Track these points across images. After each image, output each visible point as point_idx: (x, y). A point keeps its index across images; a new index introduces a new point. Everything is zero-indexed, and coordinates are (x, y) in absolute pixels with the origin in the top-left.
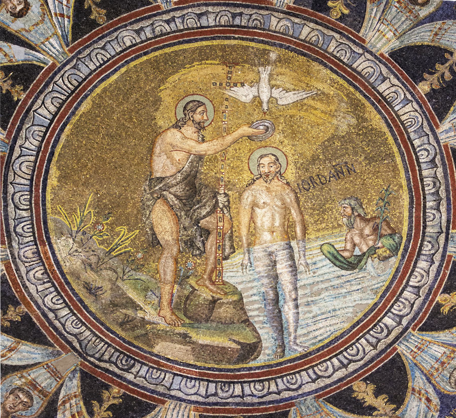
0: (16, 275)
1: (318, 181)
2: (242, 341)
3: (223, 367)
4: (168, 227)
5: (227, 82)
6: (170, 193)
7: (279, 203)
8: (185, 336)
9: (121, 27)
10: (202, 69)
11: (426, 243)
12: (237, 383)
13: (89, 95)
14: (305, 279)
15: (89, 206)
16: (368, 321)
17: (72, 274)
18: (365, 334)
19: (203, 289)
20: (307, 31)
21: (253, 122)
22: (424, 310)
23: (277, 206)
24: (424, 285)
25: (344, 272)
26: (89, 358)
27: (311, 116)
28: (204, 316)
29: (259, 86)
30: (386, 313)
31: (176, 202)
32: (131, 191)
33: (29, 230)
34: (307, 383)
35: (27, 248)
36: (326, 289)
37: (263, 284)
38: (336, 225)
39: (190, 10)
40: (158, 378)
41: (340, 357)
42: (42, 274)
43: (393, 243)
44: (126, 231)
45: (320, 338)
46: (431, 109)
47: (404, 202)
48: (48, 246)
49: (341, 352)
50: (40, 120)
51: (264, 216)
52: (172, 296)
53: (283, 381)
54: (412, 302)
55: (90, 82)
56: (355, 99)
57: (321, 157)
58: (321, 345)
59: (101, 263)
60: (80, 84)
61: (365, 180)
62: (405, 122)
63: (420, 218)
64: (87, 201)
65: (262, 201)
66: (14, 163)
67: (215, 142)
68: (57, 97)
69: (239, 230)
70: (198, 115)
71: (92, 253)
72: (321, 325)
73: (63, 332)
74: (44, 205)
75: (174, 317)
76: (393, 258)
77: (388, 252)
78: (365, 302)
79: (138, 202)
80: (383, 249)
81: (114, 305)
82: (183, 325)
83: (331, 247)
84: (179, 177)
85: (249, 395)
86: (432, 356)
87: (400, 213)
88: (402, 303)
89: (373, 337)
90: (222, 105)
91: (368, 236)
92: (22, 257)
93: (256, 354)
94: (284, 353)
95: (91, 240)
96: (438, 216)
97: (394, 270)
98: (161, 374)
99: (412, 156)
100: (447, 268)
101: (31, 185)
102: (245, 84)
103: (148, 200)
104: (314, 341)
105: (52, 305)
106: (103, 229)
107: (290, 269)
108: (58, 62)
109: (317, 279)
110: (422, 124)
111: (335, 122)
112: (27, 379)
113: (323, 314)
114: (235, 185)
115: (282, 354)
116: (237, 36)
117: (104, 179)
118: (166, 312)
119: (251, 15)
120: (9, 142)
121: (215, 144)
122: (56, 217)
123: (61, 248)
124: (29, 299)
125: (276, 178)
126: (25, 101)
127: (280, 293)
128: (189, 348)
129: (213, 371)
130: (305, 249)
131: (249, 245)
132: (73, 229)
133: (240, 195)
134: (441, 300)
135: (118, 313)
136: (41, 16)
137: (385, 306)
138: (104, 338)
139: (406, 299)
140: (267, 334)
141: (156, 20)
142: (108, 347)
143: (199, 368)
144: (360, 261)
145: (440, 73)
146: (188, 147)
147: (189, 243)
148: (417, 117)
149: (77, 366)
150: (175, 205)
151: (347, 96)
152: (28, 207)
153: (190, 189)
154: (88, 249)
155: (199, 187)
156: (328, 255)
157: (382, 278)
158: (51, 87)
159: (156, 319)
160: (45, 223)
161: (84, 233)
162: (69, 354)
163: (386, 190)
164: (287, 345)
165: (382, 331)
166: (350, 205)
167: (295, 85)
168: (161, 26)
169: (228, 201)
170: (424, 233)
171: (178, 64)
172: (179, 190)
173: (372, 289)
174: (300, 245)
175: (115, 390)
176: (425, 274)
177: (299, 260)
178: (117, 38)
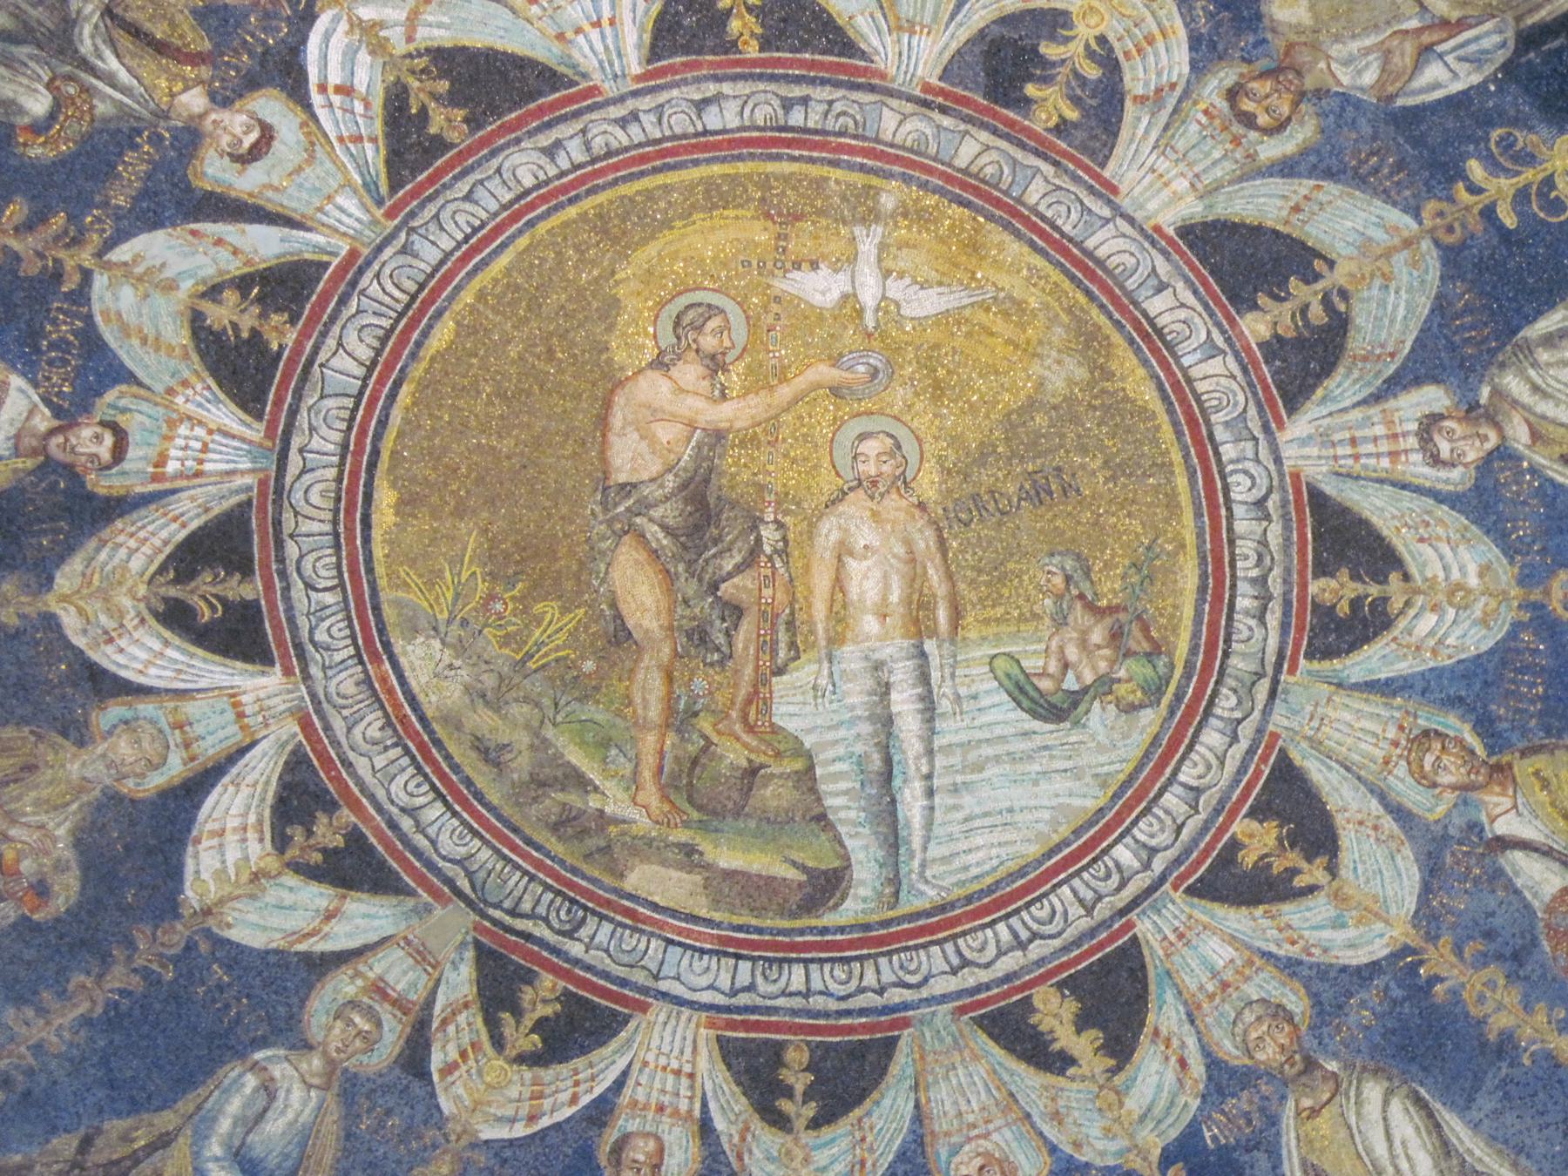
2: (810, 864)
3: (769, 923)
4: (649, 601)
6: (651, 520)
7: (900, 550)
8: (689, 850)
9: (507, 145)
11: (1224, 691)
12: (798, 960)
14: (950, 731)
18: (1072, 876)
20: (973, 149)
21: (841, 355)
25: (1037, 725)
26: (491, 911)
27: (981, 349)
28: (730, 805)
30: (1122, 836)
35: (343, 675)
36: (997, 759)
39: (675, 92)
41: (1014, 921)
42: (382, 729)
45: (975, 871)
49: (1017, 911)
51: (865, 577)
55: (446, 279)
58: (976, 887)
60: (422, 286)
67: (752, 400)
71: (484, 667)
72: (980, 841)
73: (435, 857)
74: (370, 570)
75: (666, 807)
76: (1149, 711)
78: (1077, 802)
82: (686, 825)
84: (670, 482)
86: (1204, 961)
91: (1099, 647)
96: (1259, 633)
97: (1147, 738)
100: (1264, 759)
101: (336, 535)
103: (604, 538)
104: (962, 876)
105: (406, 798)
109: (979, 735)
111: (1036, 369)
112: (364, 977)
113: (986, 814)
114: (798, 504)
116: (797, 153)
118: (650, 795)
119: (830, 103)
122: (400, 594)
124: (356, 790)
127: (896, 758)
133: (812, 525)
137: (1119, 818)
139: (1167, 812)
144: (1075, 705)
146: (687, 413)
151: (1069, 311)
156: (1006, 682)
157: (1122, 753)
159: (631, 812)
160: (377, 609)
161: (464, 623)
163: (1149, 548)
165: (1108, 876)
168: (605, 133)
169: (785, 539)
172: (669, 512)
175: (547, 980)
176: (1214, 762)
178: (498, 171)
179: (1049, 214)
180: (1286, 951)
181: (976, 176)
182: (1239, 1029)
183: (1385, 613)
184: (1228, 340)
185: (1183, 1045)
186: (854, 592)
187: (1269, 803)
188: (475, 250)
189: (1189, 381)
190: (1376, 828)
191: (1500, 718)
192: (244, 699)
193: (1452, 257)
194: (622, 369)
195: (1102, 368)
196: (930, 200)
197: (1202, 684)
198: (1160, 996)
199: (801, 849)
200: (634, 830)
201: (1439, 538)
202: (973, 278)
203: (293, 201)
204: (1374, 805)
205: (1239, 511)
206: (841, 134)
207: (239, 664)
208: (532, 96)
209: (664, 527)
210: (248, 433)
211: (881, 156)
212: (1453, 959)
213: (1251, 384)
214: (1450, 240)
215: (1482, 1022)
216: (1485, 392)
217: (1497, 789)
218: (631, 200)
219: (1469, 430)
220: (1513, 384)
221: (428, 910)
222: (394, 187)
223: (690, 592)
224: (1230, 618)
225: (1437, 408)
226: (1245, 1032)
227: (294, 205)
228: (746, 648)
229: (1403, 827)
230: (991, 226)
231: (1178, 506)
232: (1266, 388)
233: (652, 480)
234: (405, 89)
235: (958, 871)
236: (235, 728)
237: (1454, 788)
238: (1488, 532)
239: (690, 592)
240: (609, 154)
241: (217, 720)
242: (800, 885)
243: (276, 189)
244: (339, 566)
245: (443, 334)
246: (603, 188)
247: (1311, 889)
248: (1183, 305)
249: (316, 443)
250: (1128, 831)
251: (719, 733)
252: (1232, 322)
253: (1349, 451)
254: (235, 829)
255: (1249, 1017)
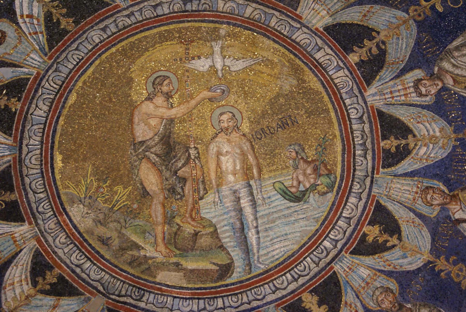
0: (47, 246)
1: (268, 132)
3: (208, 285)
4: (154, 181)
5: (186, 57)
6: (151, 153)
7: (238, 151)
8: (177, 265)
9: (89, 29)
10: (163, 49)
11: (355, 183)
12: (220, 297)
13: (73, 89)
14: (262, 210)
15: (90, 176)
16: (312, 244)
17: (87, 232)
18: (310, 254)
19: (186, 225)
21: (211, 87)
22: (354, 237)
23: (237, 153)
24: (354, 217)
25: (292, 204)
26: (111, 296)
27: (259, 78)
28: (190, 247)
29: (213, 58)
30: (325, 238)
31: (157, 160)
32: (120, 156)
33: (48, 207)
34: (269, 294)
36: (279, 218)
37: (231, 216)
38: (284, 167)
40: (162, 302)
43: (330, 181)
44: (122, 189)
45: (277, 257)
46: (360, 76)
47: (337, 148)
48: (65, 215)
49: (293, 269)
50: (37, 119)
51: (227, 162)
52: (164, 234)
53: (251, 292)
54: (345, 230)
55: (72, 78)
56: (295, 64)
57: (269, 112)
58: (278, 262)
59: (107, 218)
60: (63, 82)
61: (306, 130)
62: (338, 84)
63: (351, 163)
64: (88, 172)
65: (225, 151)
66: (24, 160)
67: (182, 107)
68: (47, 98)
69: (209, 175)
70: (165, 87)
71: (99, 212)
72: (277, 246)
74: (55, 184)
75: (168, 251)
76: (330, 194)
77: (326, 188)
78: (308, 228)
79: (127, 164)
80: (322, 186)
81: (123, 249)
82: (175, 256)
83: (281, 184)
84: (157, 139)
85: (229, 307)
87: (335, 157)
88: (337, 230)
89: (316, 256)
90: (184, 76)
91: (310, 175)
92: (48, 230)
93: (230, 272)
94: (251, 270)
95: (97, 202)
97: (330, 203)
98: (164, 299)
99: (344, 112)
100: (371, 205)
101: (42, 172)
102: (202, 57)
103: (136, 161)
104: (272, 259)
105: (77, 261)
106: (104, 191)
107: (251, 203)
108: (41, 70)
109: (272, 210)
110: (352, 87)
111: (279, 82)
113: (277, 237)
115: (249, 271)
116: (190, 19)
117: (98, 151)
118: (162, 247)
120: (17, 145)
121: (182, 108)
122: (67, 190)
123: (75, 214)
125: (234, 131)
126: (22, 111)
127: (245, 222)
128: (182, 274)
129: (201, 290)
130: (261, 186)
131: (218, 186)
132: (81, 196)
133: (207, 147)
134: (367, 230)
135: (126, 255)
136: (18, 39)
137: (324, 232)
138: (119, 277)
140: (237, 255)
141: (118, 17)
142: (123, 284)
143: (191, 289)
144: (304, 195)
145: (368, 47)
146: (160, 114)
147: (171, 191)
148: (348, 81)
149: (104, 305)
150: (157, 162)
151: (288, 61)
152: (44, 189)
153: (167, 147)
154: (95, 209)
155: (173, 145)
156: (279, 191)
157: (322, 209)
158: (40, 91)
159: (156, 255)
160: (59, 197)
161: (90, 197)
162: (97, 297)
163: (323, 139)
164: (253, 264)
165: (322, 252)
166: (295, 150)
167: (244, 55)
168: (123, 21)
169: (198, 153)
170: (354, 175)
171: (143, 48)
172: (158, 149)
173: (314, 218)
174: (257, 184)
177: (257, 196)
178: (86, 38)
179: (279, 29)
180: (387, 268)
181: (252, 19)
182: (375, 298)
183: (408, 149)
184: (344, 64)
185: (356, 306)
186: (224, 168)
187: (375, 219)
188: (82, 67)
189: (332, 80)
190: (413, 222)
191: (452, 179)
192: (16, 235)
193: (420, 24)
194: (136, 102)
195: (301, 79)
196: (237, 30)
197: (347, 181)
198: (346, 290)
199: (216, 258)
200: (158, 260)
201: (425, 121)
202: (254, 55)
203: (15, 58)
204: (412, 214)
205: (353, 121)
206: (204, 11)
207: (13, 223)
208: (96, 11)
209: (156, 155)
210: (7, 142)
211: (219, 16)
212: (446, 263)
213: (354, 78)
214: (420, 19)
215: (460, 283)
216: (436, 69)
217: (454, 203)
218: (134, 43)
219: (431, 83)
220: (446, 65)
221: (89, 299)
222: (50, 49)
223: (168, 176)
224: (354, 158)
225: (419, 77)
226: (377, 298)
227: (15, 59)
228: (189, 192)
229: (422, 221)
230: (259, 36)
231: (333, 123)
232: (359, 78)
233: (151, 139)
234: (51, 13)
235: (270, 258)
236: (14, 246)
237: (439, 205)
238: (441, 117)
239: (168, 176)
240: (125, 28)
241: (7, 244)
242: (217, 271)
243: (9, 54)
244: (44, 184)
245: (73, 98)
246: (123, 40)
247: (394, 246)
248: (328, 54)
249: (32, 142)
250: (327, 236)
251: (183, 223)
252: (345, 58)
253: (390, 96)
254: (18, 282)
255: (377, 293)
